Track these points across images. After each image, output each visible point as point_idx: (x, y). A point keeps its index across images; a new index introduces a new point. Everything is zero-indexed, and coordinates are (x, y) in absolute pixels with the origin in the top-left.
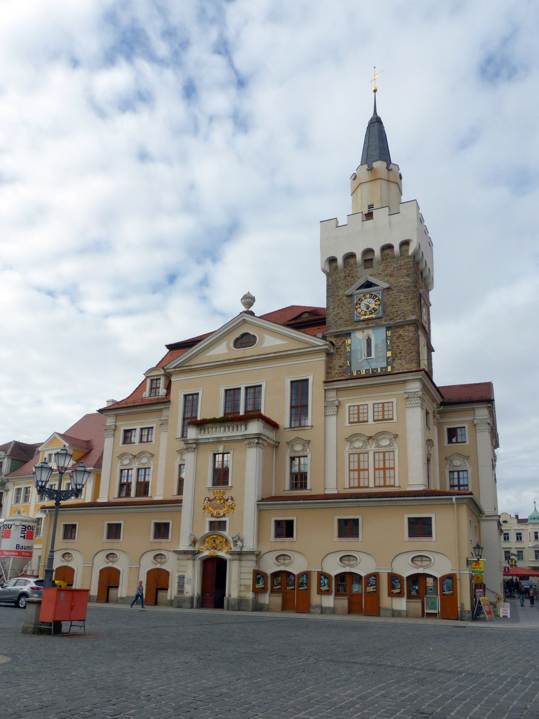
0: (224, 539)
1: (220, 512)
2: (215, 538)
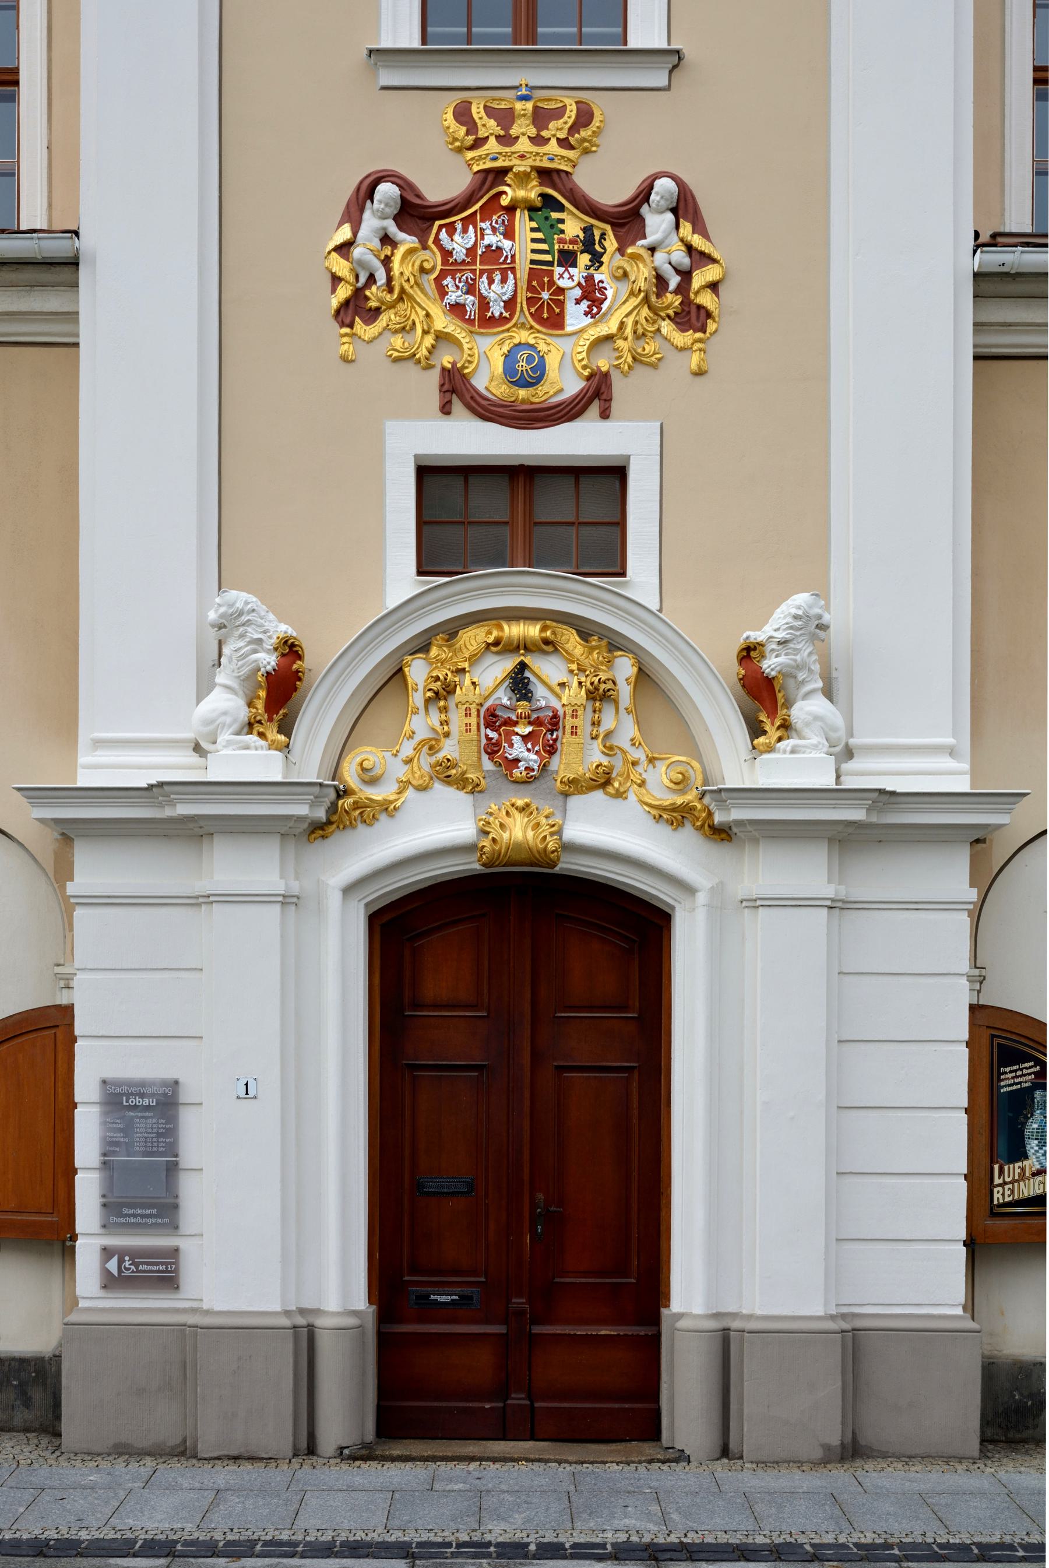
0: (625, 668)
1: (552, 362)
2: (525, 646)
